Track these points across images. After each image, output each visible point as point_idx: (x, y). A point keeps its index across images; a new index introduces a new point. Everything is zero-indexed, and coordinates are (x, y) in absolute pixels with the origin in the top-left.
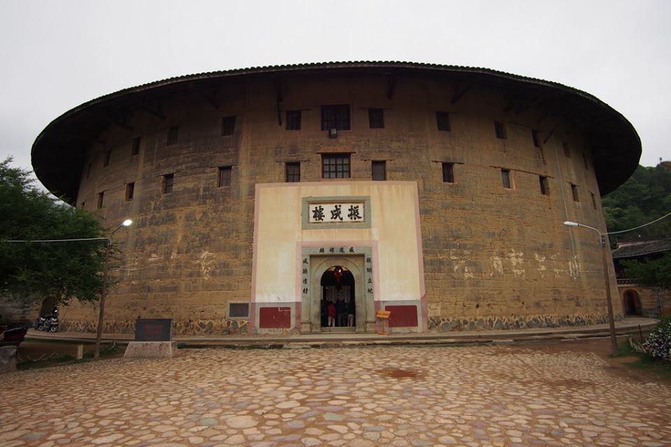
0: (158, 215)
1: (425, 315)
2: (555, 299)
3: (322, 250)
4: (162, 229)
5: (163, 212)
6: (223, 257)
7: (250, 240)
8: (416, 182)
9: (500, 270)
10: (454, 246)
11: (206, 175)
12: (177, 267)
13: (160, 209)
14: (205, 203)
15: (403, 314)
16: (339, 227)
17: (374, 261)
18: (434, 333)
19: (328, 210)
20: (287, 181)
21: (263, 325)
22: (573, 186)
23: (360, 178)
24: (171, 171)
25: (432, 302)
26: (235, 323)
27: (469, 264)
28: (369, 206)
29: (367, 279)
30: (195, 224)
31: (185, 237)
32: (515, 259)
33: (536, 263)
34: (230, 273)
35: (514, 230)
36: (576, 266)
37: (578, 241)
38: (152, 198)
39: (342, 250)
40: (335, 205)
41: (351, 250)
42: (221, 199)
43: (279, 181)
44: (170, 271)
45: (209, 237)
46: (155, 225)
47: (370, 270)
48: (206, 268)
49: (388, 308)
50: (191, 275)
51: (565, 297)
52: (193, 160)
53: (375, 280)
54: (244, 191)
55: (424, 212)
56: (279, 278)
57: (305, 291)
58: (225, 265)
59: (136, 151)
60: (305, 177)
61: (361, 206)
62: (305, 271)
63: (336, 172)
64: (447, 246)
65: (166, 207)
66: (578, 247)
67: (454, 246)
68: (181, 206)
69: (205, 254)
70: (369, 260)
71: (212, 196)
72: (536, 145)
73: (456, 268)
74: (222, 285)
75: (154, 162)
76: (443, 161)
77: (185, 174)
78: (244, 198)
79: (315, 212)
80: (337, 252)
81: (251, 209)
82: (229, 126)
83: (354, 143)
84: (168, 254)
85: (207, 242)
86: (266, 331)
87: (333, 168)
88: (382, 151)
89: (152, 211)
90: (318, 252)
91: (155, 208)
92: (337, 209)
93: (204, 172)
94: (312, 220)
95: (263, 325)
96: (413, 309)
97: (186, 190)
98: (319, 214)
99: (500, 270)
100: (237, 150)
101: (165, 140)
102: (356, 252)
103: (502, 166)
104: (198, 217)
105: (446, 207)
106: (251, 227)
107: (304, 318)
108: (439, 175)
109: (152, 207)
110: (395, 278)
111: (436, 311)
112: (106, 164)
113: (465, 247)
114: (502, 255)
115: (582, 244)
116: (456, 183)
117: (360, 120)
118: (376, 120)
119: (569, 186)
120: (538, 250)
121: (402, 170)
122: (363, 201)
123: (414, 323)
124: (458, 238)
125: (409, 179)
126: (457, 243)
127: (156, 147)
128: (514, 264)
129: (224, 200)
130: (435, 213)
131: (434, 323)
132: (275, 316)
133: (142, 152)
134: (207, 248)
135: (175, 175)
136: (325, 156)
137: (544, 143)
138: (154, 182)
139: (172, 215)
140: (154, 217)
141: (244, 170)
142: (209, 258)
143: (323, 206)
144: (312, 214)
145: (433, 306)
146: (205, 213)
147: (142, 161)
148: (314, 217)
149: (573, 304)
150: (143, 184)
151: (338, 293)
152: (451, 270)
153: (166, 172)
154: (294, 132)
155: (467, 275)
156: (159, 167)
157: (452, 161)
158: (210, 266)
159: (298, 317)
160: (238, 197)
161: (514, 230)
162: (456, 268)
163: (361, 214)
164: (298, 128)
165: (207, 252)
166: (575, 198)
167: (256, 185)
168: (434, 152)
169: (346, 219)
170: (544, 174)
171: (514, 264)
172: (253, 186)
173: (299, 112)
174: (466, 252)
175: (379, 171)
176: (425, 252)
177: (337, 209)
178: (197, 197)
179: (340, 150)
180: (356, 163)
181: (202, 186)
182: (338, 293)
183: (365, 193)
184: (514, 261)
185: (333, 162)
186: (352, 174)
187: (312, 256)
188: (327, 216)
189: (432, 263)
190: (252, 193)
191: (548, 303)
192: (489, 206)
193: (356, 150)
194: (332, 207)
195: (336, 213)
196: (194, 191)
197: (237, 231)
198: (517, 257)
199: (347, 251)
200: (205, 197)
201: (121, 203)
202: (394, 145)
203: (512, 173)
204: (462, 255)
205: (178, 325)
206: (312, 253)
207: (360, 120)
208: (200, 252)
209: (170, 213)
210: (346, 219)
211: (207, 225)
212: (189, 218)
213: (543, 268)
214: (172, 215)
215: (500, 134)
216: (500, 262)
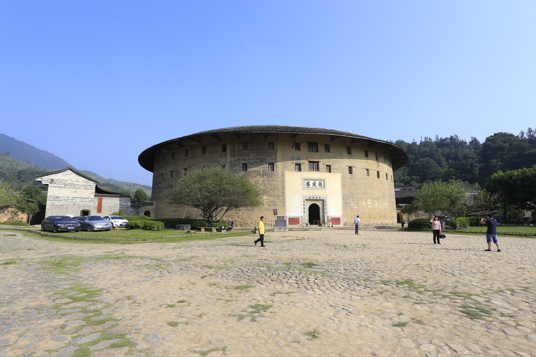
7: (284, 193)
14: (263, 177)
15: (336, 221)
18: (345, 227)
23: (322, 171)
24: (246, 162)
32: (369, 202)
33: (375, 203)
35: (369, 192)
52: (256, 159)
54: (280, 173)
55: (343, 186)
56: (296, 208)
57: (304, 212)
58: (274, 202)
59: (224, 150)
64: (350, 197)
69: (265, 197)
71: (266, 174)
72: (377, 159)
77: (253, 164)
82: (272, 145)
94: (306, 186)
96: (339, 219)
98: (308, 184)
100: (276, 157)
102: (321, 199)
106: (283, 188)
108: (348, 171)
112: (204, 152)
114: (366, 201)
117: (321, 148)
118: (327, 149)
123: (339, 224)
132: (294, 221)
133: (228, 151)
136: (310, 162)
141: (279, 165)
151: (315, 214)
153: (243, 162)
154: (299, 152)
156: (239, 159)
161: (369, 192)
163: (323, 185)
166: (387, 179)
168: (346, 162)
172: (284, 172)
173: (299, 144)
175: (329, 168)
176: (343, 199)
178: (260, 174)
180: (321, 165)
182: (315, 214)
185: (312, 164)
186: (320, 169)
187: (306, 200)
188: (311, 185)
190: (283, 175)
195: (314, 184)
197: (278, 189)
199: (318, 198)
200: (263, 175)
207: (321, 148)
211: (265, 186)
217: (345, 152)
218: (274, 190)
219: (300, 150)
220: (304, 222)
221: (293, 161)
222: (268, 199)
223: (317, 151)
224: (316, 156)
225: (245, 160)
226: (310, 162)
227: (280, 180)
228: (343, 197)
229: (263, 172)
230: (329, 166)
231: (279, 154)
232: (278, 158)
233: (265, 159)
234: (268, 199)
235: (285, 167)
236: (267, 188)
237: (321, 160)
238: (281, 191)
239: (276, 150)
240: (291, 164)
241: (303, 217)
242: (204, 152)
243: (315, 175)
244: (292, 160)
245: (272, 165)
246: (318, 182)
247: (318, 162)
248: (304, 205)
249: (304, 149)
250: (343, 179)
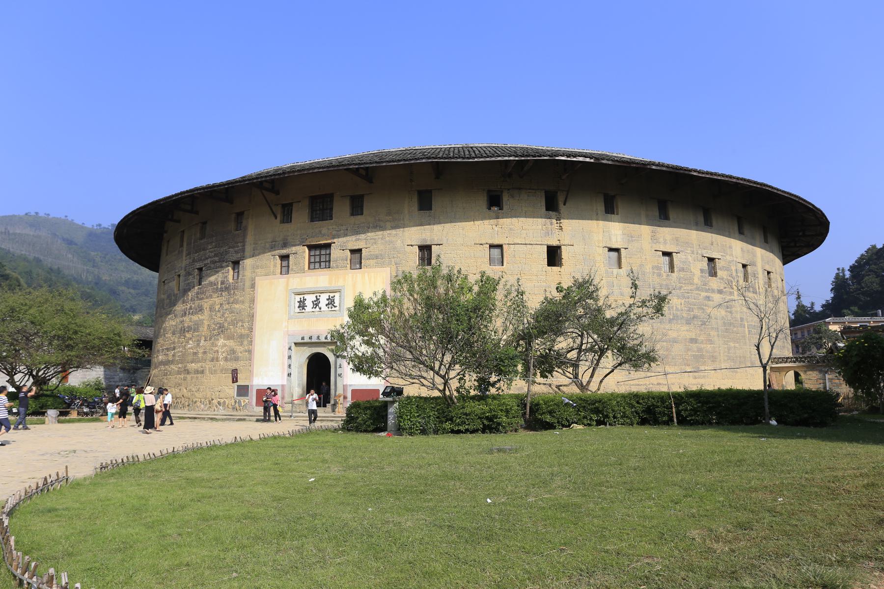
3: (303, 338)
4: (195, 318)
6: (231, 343)
12: (205, 353)
19: (310, 299)
26: (240, 402)
39: (318, 337)
44: (200, 355)
49: (354, 391)
57: (289, 375)
58: (233, 351)
61: (337, 295)
63: (320, 262)
68: (207, 298)
69: (221, 342)
71: (227, 289)
76: (419, 244)
78: (248, 290)
80: (314, 340)
81: (253, 301)
83: (334, 233)
84: (199, 341)
87: (317, 260)
90: (301, 341)
92: (318, 299)
94: (298, 310)
98: (302, 305)
101: (198, 235)
103: (491, 242)
104: (217, 307)
106: (252, 317)
117: (341, 208)
121: (377, 257)
125: (382, 265)
141: (248, 263)
142: (225, 345)
143: (306, 296)
144: (298, 304)
146: (221, 304)
147: (184, 254)
156: (194, 261)
157: (428, 243)
159: (283, 398)
160: (243, 290)
163: (336, 304)
169: (324, 308)
173: (291, 205)
177: (318, 299)
180: (335, 252)
183: (338, 284)
185: (318, 252)
190: (253, 286)
194: (312, 298)
195: (316, 303)
200: (222, 290)
210: (324, 308)
212: (211, 309)
217: (411, 205)
218: (234, 323)
221: (273, 253)
224: (324, 231)
225: (200, 260)
226: (311, 247)
229: (222, 283)
230: (357, 252)
232: (249, 248)
233: (227, 252)
235: (258, 267)
237: (335, 240)
239: (246, 229)
240: (271, 261)
241: (287, 389)
243: (320, 279)
244: (273, 248)
245: (236, 264)
247: (328, 246)
248: (290, 357)
249: (300, 215)
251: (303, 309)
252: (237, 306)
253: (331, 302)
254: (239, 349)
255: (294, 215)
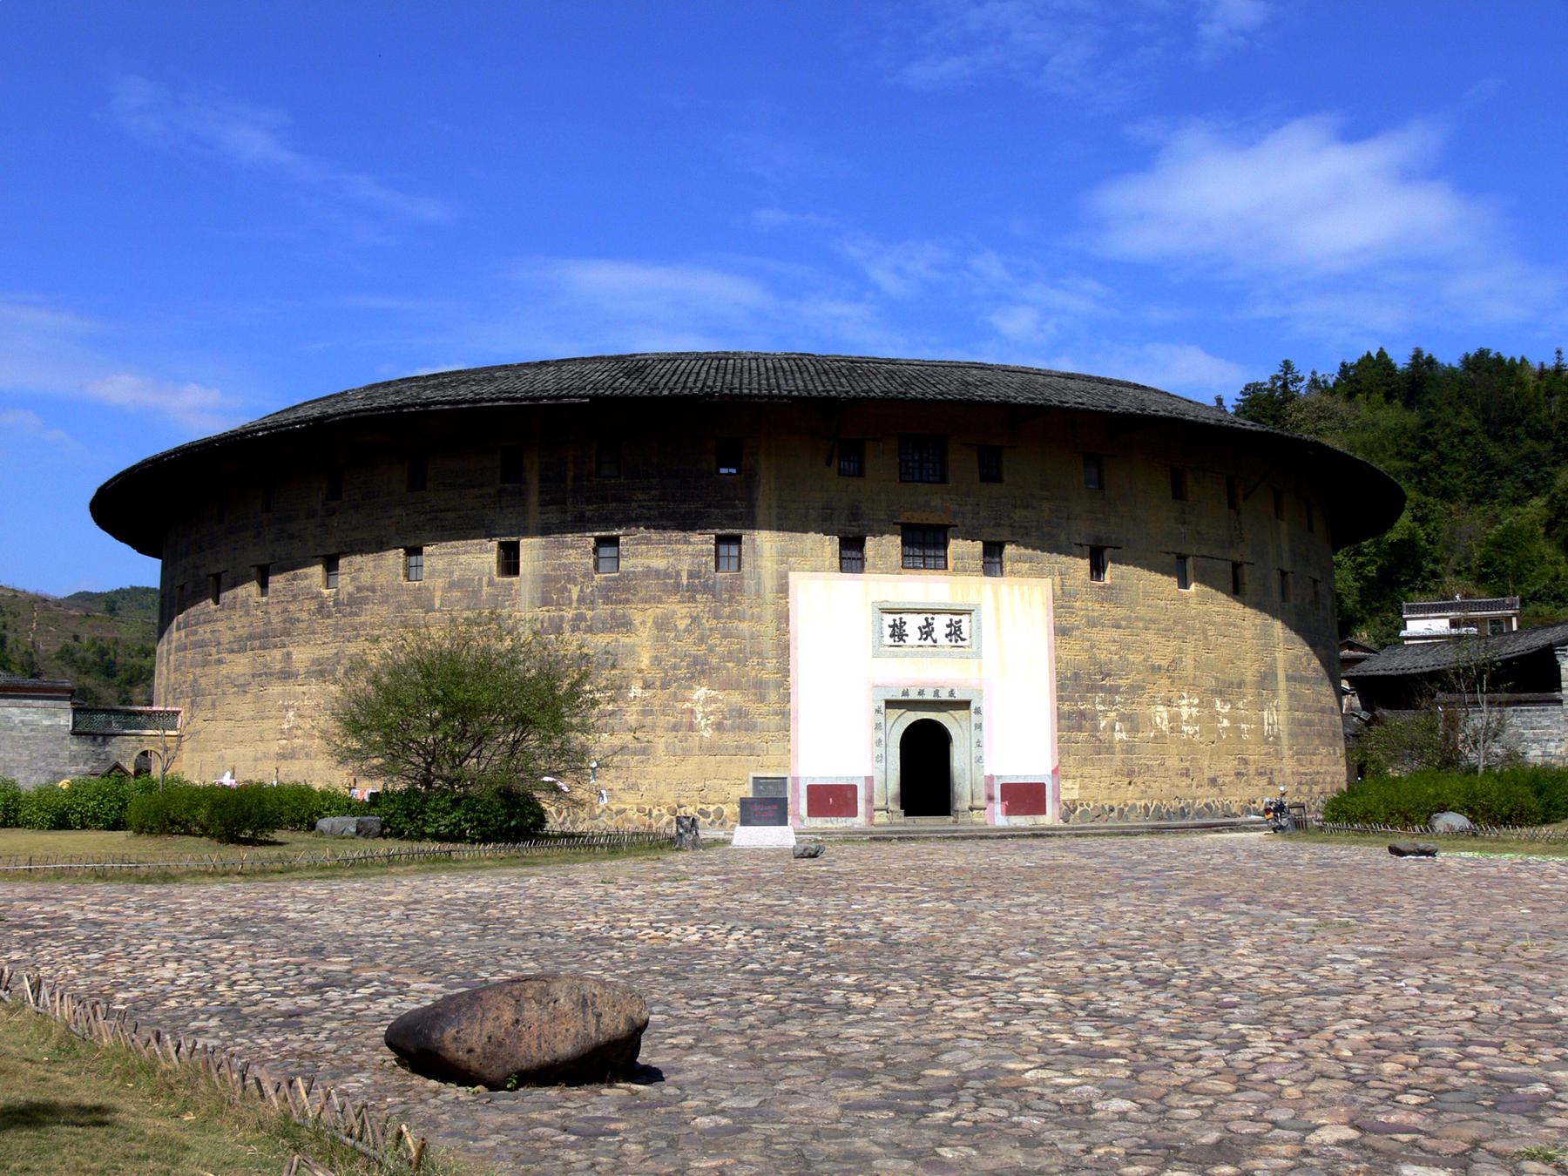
0: (589, 614)
1: (1057, 799)
2: (1238, 774)
3: (905, 693)
4: (601, 640)
5: (603, 610)
6: (736, 698)
8: (1049, 581)
9: (1165, 726)
10: (1102, 688)
11: (690, 548)
12: (645, 713)
13: (592, 602)
14: (692, 599)
15: (1025, 797)
16: (933, 655)
17: (983, 711)
20: (841, 570)
21: (813, 812)
22: (1283, 574)
25: (1067, 777)
27: (1123, 718)
28: (979, 621)
29: (974, 741)
30: (677, 638)
31: (657, 660)
33: (1215, 717)
34: (751, 728)
36: (1276, 718)
37: (1281, 675)
38: (574, 581)
39: (936, 693)
40: (923, 616)
41: (952, 693)
42: (725, 596)
43: (830, 569)
45: (706, 662)
46: (586, 632)
47: (979, 726)
48: (706, 716)
49: (1005, 787)
50: (675, 728)
51: (1252, 769)
53: (985, 743)
54: (769, 584)
56: (840, 738)
58: (741, 713)
59: (513, 473)
60: (874, 566)
61: (965, 618)
62: (878, 727)
64: (1093, 689)
65: (608, 600)
66: (1282, 684)
67: (1102, 688)
69: (701, 693)
70: (978, 711)
71: (707, 589)
72: (1233, 505)
73: (1103, 724)
74: (738, 747)
75: (570, 507)
78: (769, 596)
79: (893, 626)
80: (929, 696)
81: (784, 618)
85: (703, 672)
86: (819, 823)
88: (999, 525)
89: (575, 605)
90: (900, 697)
91: (581, 600)
92: (929, 624)
93: (687, 542)
95: (813, 812)
97: (650, 573)
98: (898, 632)
99: (1165, 726)
100: (751, 506)
102: (959, 697)
104: (682, 624)
105: (1092, 623)
106: (784, 649)
107: (878, 803)
109: (575, 597)
110: (1010, 739)
111: (1071, 791)
112: (417, 482)
113: (1114, 690)
114: (1168, 703)
115: (1289, 678)
116: (1108, 581)
117: (962, 463)
119: (1276, 575)
120: (1220, 693)
122: (969, 612)
123: (1040, 809)
124: (1109, 675)
126: (1107, 682)
127: (570, 475)
128: (1185, 717)
129: (731, 599)
130: (1077, 633)
131: (1069, 810)
134: (704, 681)
135: (622, 540)
137: (1245, 498)
138: (573, 547)
139: (624, 615)
140: (580, 617)
142: (709, 701)
143: (905, 617)
145: (1069, 784)
146: (694, 619)
148: (892, 636)
149: (1264, 781)
150: (545, 548)
152: (1096, 728)
155: (1118, 736)
158: (712, 713)
159: (870, 801)
160: (758, 594)
162: (1103, 724)
164: (860, 473)
165: (704, 689)
167: (791, 575)
170: (1238, 559)
171: (1185, 717)
172: (786, 577)
174: (1118, 698)
176: (1060, 699)
177: (929, 624)
178: (678, 585)
179: (934, 519)
181: (685, 566)
184: (1185, 712)
189: (1069, 716)
190: (783, 589)
191: (1227, 780)
192: (1154, 621)
193: (957, 522)
194: (920, 620)
195: (927, 631)
196: (668, 576)
197: (760, 655)
198: (1190, 705)
199: (944, 696)
200: (692, 590)
201: (485, 579)
202: (1019, 514)
203: (1190, 561)
204: (1113, 703)
205: (655, 812)
206: (889, 697)
207: (962, 463)
208: (691, 688)
209: (619, 612)
211: (702, 640)
212: (662, 625)
213: (1226, 723)
214: (624, 615)
215: (1178, 493)
216: (1165, 715)
219: (860, 473)
220: (878, 803)
222: (714, 700)
223: (943, 480)
227: (769, 612)
228: (1061, 687)
229: (691, 575)
231: (765, 501)
232: (761, 513)
234: (714, 700)
236: (711, 650)
238: (772, 663)
242: (417, 482)
246: (946, 619)
249: (881, 465)
250: (1062, 602)
251: (901, 639)
252: (744, 626)
253: (955, 632)
254: (754, 708)
255: (868, 466)
